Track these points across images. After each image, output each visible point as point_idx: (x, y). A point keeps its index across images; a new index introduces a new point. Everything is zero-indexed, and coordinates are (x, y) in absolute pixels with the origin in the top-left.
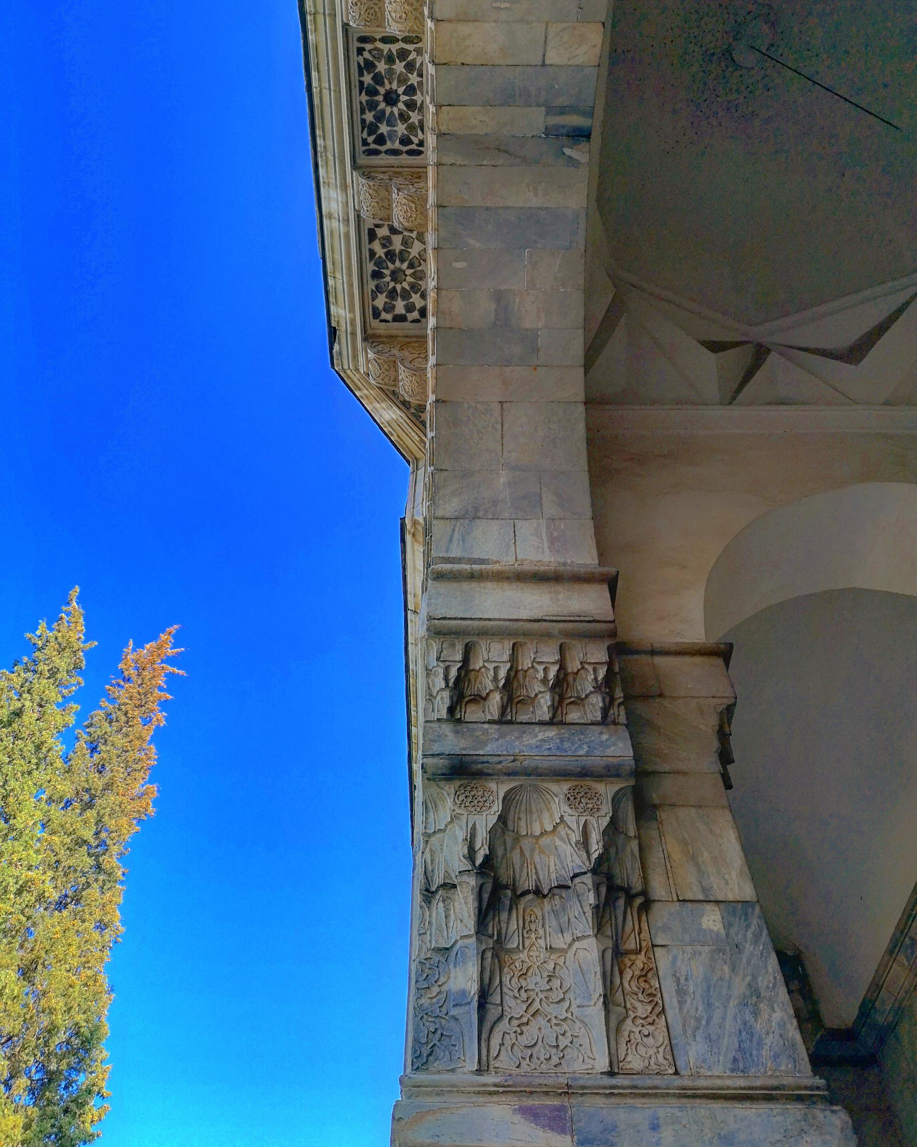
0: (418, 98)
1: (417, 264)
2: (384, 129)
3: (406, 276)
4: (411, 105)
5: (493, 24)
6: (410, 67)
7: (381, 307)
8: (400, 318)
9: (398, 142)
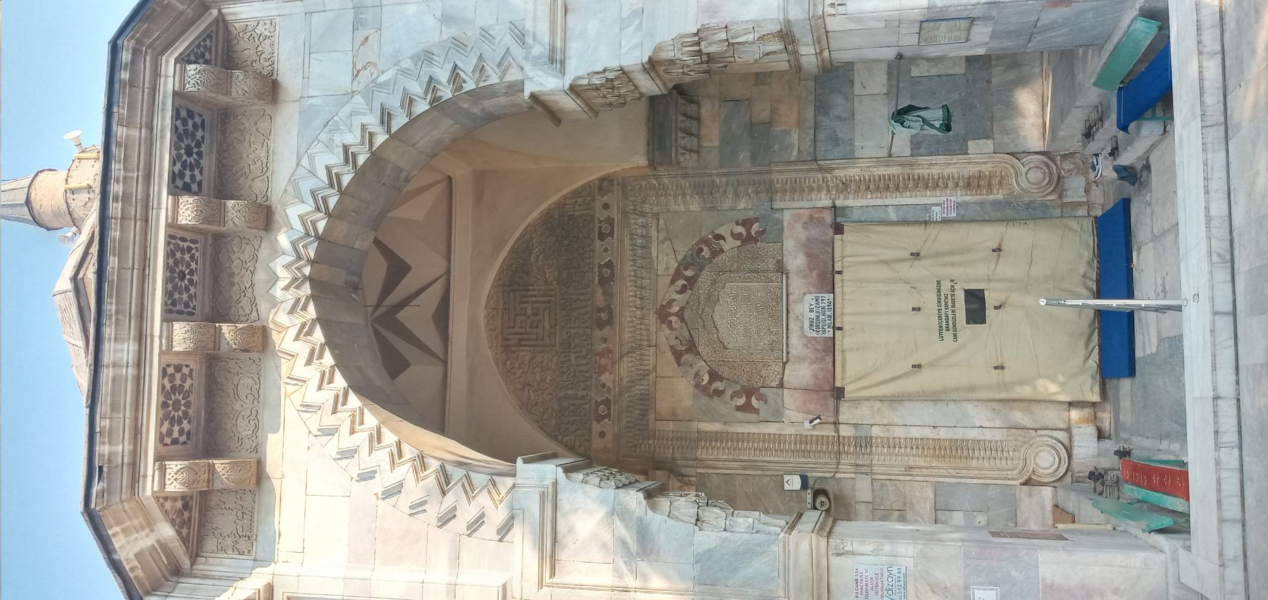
0: (195, 278)
1: (186, 396)
2: (176, 296)
3: (181, 405)
4: (191, 281)
5: (345, 223)
6: (192, 257)
7: (165, 432)
8: (175, 442)
9: (182, 305)
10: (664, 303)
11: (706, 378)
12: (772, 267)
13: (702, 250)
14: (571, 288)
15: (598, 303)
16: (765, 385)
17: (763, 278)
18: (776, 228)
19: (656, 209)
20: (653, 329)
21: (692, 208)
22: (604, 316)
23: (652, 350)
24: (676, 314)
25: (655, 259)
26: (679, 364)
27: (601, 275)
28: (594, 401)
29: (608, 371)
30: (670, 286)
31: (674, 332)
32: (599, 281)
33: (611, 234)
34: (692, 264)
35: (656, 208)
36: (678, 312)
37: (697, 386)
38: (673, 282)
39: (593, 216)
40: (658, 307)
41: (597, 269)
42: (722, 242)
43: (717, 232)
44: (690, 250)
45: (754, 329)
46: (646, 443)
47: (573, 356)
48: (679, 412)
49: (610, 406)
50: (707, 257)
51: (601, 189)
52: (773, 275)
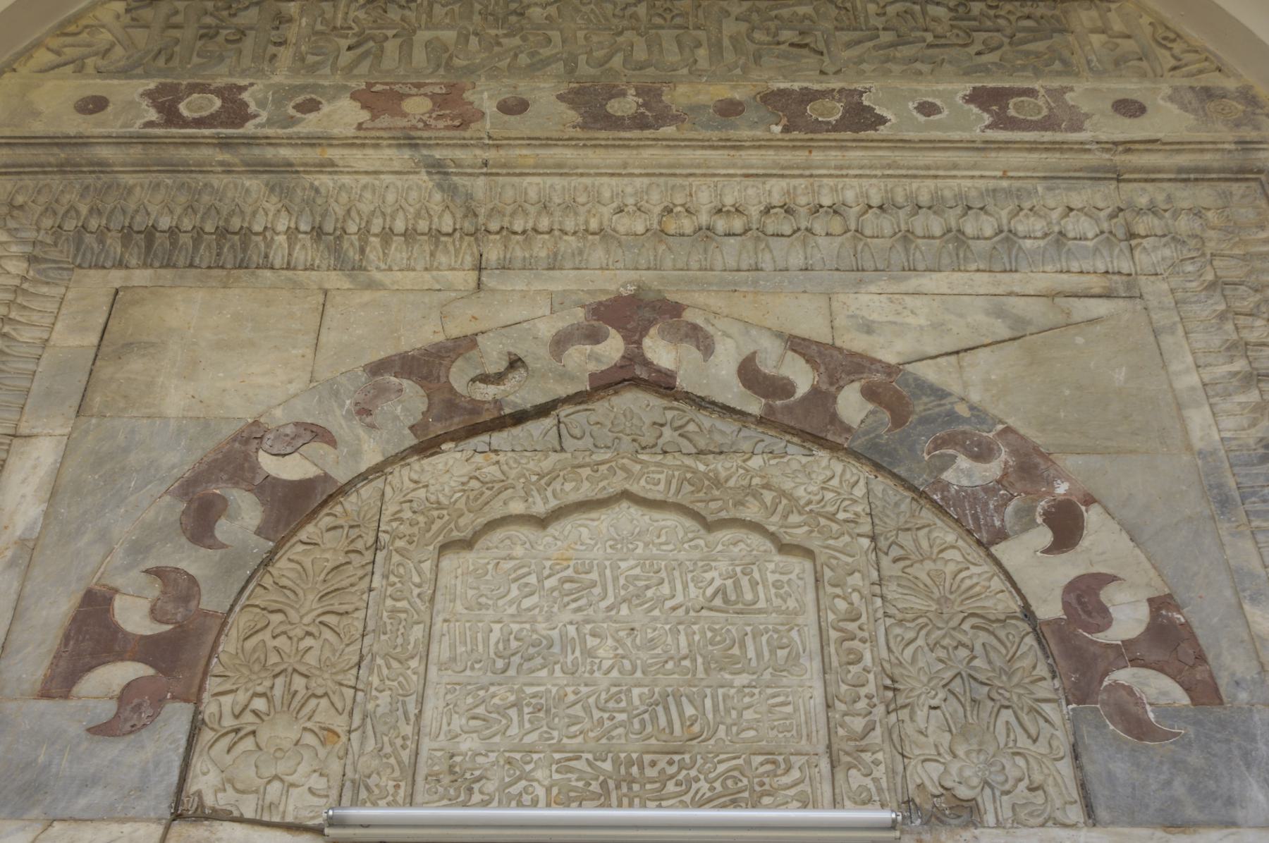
10: (689, 316)
11: (292, 469)
12: (928, 775)
13: (982, 453)
14: (743, 27)
15: (682, 89)
16: (207, 736)
17: (858, 724)
18: (1179, 788)
19: (1156, 289)
20: (563, 281)
21: (1198, 420)
22: (625, 105)
23: (464, 279)
24: (634, 358)
25: (904, 287)
26: (377, 369)
27: (808, 96)
28: (243, 82)
29: (374, 118)
30: (779, 335)
31: (544, 352)
32: (782, 93)
33: (1003, 122)
34: (899, 420)
35: (1165, 286)
36: (647, 363)
37: (253, 435)
38: (797, 345)
39: (1068, 69)
40: (673, 297)
41: (836, 84)
42: (1044, 536)
43: (1093, 516)
44: (972, 408)
45: (549, 681)
46: (14, 249)
47: (449, 36)
48: (136, 365)
49: (212, 126)
50: (948, 476)
51: (1208, 94)
52: (880, 772)
